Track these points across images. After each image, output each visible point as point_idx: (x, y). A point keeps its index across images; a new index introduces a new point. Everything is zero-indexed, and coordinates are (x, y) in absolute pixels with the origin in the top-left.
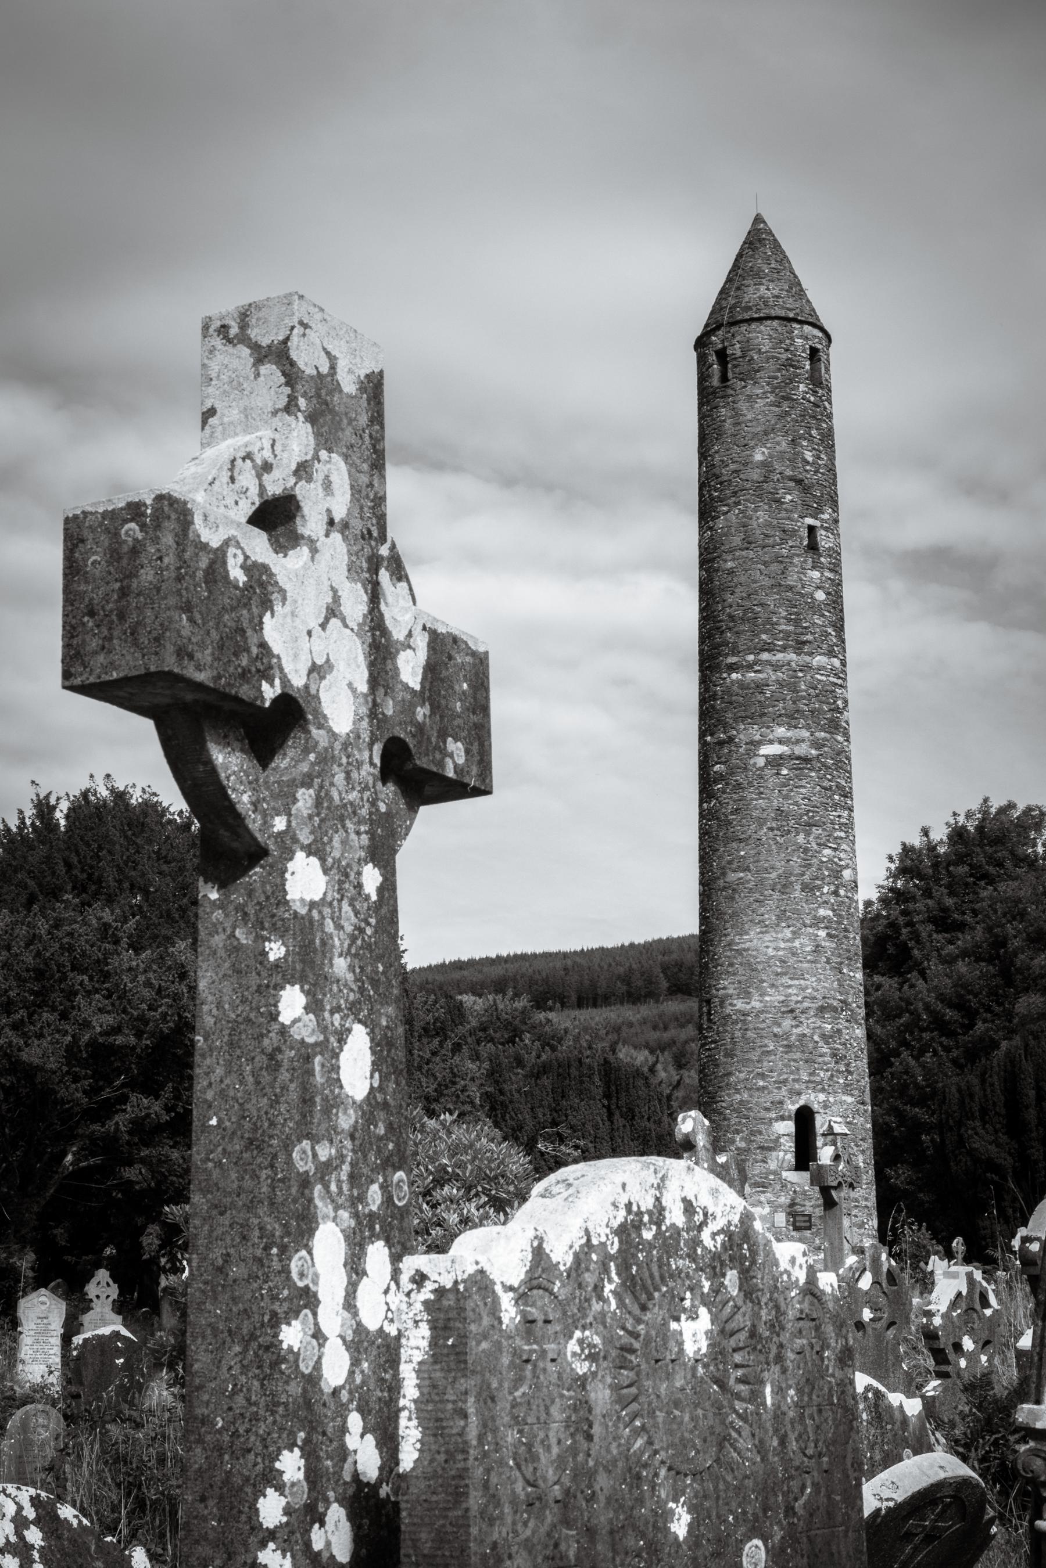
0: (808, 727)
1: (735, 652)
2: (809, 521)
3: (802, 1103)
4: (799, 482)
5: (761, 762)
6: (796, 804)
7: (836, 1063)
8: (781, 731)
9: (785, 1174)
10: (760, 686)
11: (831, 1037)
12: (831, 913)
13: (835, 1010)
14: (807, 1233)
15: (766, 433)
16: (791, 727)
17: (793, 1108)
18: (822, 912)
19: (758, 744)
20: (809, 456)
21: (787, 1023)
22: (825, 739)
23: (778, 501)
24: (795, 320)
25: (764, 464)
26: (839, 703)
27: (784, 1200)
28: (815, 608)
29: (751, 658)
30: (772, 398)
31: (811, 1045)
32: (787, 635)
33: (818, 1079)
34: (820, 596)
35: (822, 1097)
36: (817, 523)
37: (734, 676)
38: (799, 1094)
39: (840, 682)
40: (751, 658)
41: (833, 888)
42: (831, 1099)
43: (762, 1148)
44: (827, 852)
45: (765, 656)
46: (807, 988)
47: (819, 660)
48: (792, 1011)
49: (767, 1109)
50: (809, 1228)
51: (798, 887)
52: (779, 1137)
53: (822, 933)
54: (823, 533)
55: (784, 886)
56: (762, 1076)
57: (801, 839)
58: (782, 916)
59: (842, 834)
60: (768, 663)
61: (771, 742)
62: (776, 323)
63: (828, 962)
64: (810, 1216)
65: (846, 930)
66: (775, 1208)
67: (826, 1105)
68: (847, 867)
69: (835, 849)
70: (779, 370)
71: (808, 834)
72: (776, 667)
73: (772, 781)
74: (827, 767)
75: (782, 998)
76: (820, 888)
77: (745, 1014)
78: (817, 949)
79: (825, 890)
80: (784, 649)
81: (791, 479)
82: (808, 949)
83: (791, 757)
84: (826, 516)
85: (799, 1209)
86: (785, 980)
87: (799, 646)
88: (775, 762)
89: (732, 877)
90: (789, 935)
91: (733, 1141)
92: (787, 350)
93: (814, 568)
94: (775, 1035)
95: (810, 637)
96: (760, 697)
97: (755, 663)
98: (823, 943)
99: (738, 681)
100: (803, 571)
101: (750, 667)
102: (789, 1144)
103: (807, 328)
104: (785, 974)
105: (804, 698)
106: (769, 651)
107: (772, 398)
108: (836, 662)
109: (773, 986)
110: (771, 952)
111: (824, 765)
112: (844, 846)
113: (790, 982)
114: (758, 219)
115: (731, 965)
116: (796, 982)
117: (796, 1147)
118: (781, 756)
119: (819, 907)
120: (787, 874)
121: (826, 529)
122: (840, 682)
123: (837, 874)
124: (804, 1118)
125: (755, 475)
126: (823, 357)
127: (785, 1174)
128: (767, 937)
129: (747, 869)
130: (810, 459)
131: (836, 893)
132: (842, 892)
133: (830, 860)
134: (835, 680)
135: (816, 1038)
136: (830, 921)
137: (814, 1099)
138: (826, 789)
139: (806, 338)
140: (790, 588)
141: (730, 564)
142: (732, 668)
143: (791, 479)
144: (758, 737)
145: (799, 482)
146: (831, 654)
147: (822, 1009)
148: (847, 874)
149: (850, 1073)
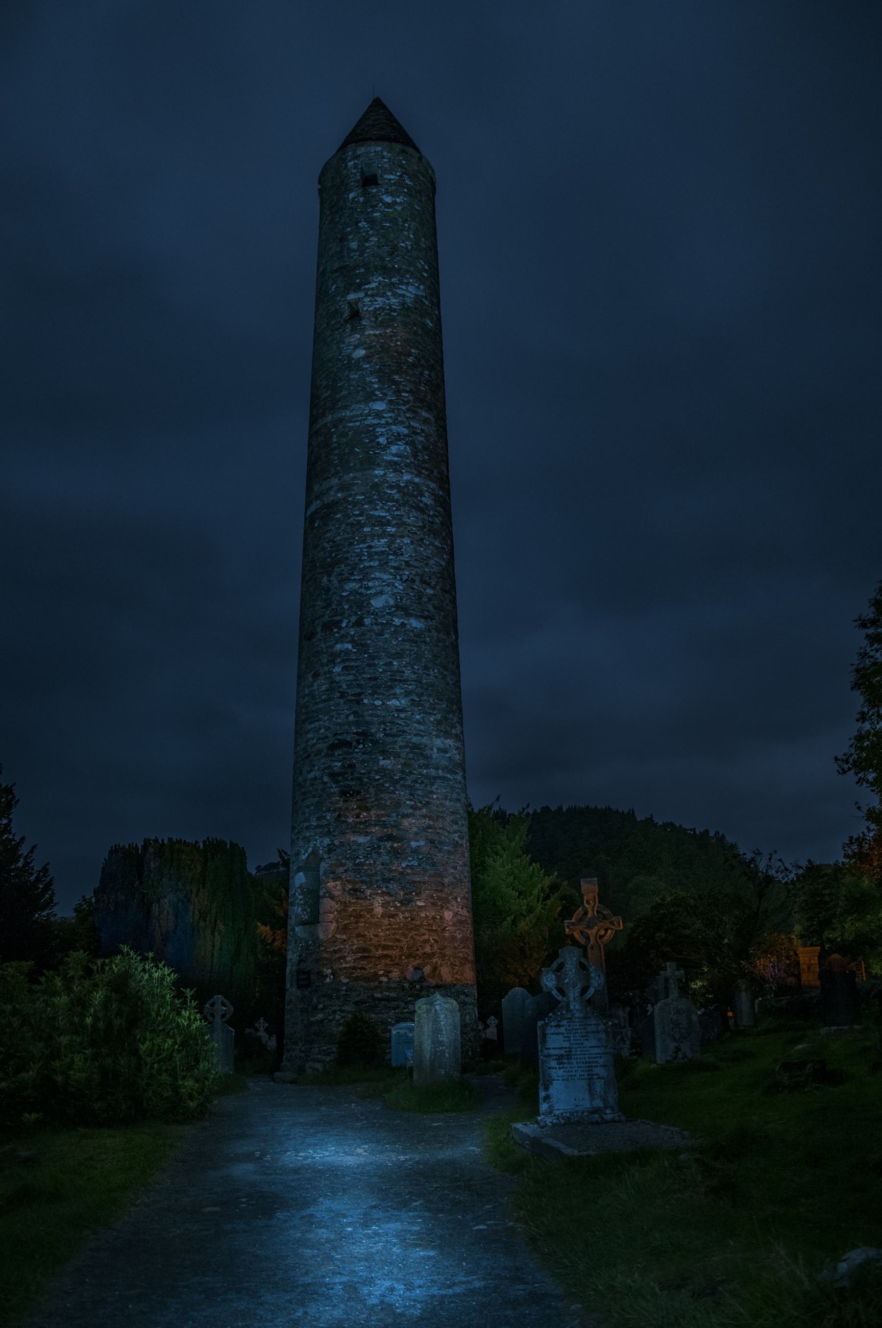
2: (352, 296)
7: (345, 801)
11: (339, 774)
12: (350, 646)
13: (348, 744)
18: (339, 647)
26: (382, 440)
33: (325, 822)
35: (327, 841)
39: (383, 421)
41: (353, 619)
42: (336, 842)
46: (320, 729)
51: (319, 629)
53: (337, 669)
54: (367, 300)
63: (343, 695)
64: (308, 973)
67: (330, 850)
69: (360, 580)
79: (344, 625)
82: (324, 688)
84: (373, 285)
90: (311, 680)
98: (338, 679)
105: (335, 448)
112: (377, 574)
113: (309, 727)
116: (313, 725)
118: (316, 512)
119: (337, 643)
122: (383, 421)
131: (359, 623)
132: (367, 621)
134: (375, 422)
135: (326, 779)
136: (347, 652)
138: (352, 525)
147: (333, 747)
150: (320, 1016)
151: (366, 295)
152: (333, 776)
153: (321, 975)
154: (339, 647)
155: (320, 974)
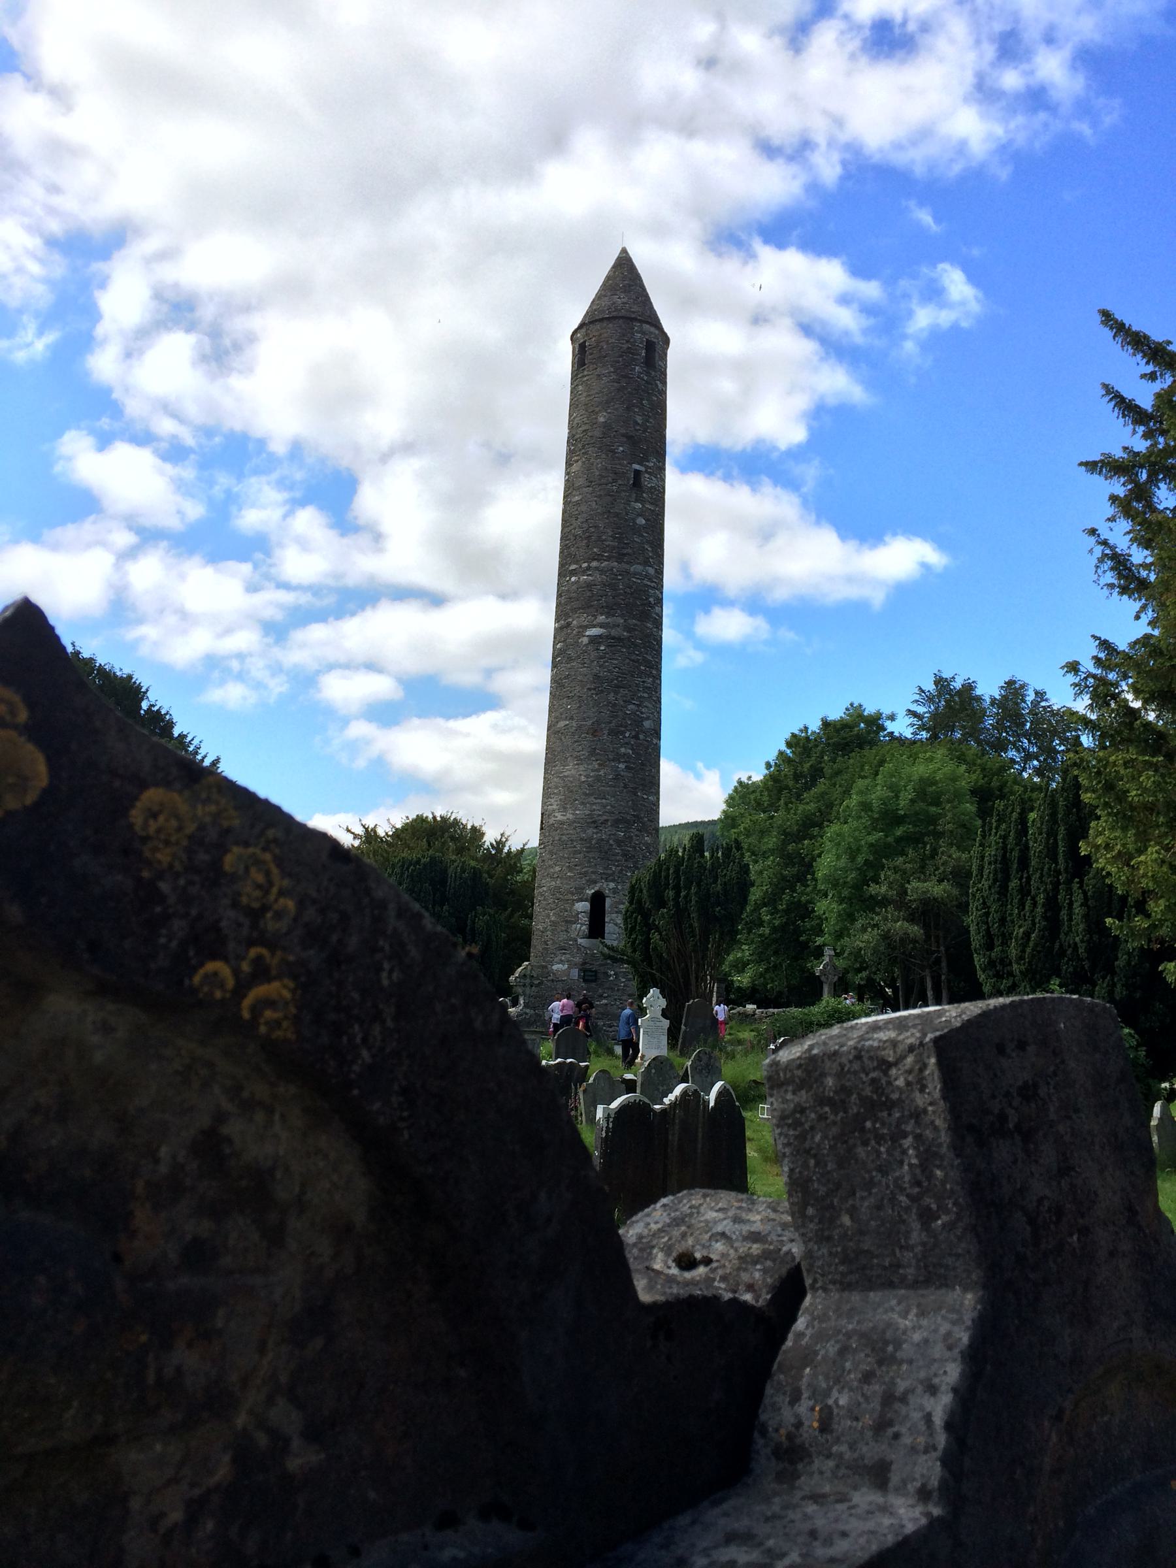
0: (622, 616)
1: (577, 562)
3: (597, 889)
4: (629, 438)
5: (585, 640)
6: (609, 671)
8: (602, 618)
9: (579, 941)
10: (589, 586)
14: (593, 985)
15: (607, 402)
16: (608, 615)
17: (590, 892)
18: (623, 750)
19: (586, 627)
20: (639, 419)
21: (590, 831)
22: (635, 625)
23: (613, 451)
24: (635, 319)
25: (607, 426)
27: (578, 960)
28: (636, 530)
29: (585, 565)
30: (614, 376)
31: (606, 848)
32: (614, 548)
33: (610, 872)
34: (641, 521)
35: (612, 885)
36: (643, 469)
37: (573, 579)
38: (595, 882)
40: (585, 565)
43: (567, 922)
44: (631, 707)
45: (594, 564)
47: (638, 568)
48: (594, 822)
49: (573, 894)
50: (595, 981)
51: (606, 732)
52: (578, 913)
53: (622, 766)
55: (596, 731)
56: (570, 869)
57: (611, 697)
58: (593, 752)
59: (646, 695)
60: (596, 568)
61: (594, 626)
62: (621, 321)
65: (642, 764)
66: (572, 965)
68: (648, 718)
70: (621, 356)
71: (616, 693)
72: (602, 571)
73: (594, 654)
74: (636, 645)
75: (587, 812)
76: (623, 733)
77: (562, 823)
78: (617, 777)
80: (609, 559)
81: (623, 435)
83: (609, 637)
85: (588, 966)
86: (592, 799)
87: (620, 557)
88: (594, 640)
89: (562, 724)
91: (548, 916)
92: (628, 342)
93: (636, 501)
94: (582, 839)
95: (630, 551)
96: (589, 594)
97: (588, 568)
99: (575, 582)
100: (628, 502)
101: (584, 572)
102: (584, 919)
103: (646, 327)
104: (591, 795)
105: (621, 594)
106: (598, 560)
107: (614, 376)
108: (651, 571)
109: (582, 803)
110: (583, 779)
111: (633, 643)
112: (646, 704)
114: (624, 251)
115: (557, 787)
117: (590, 921)
118: (600, 636)
120: (598, 722)
121: (649, 473)
123: (638, 722)
124: (598, 901)
125: (597, 433)
126: (658, 347)
127: (579, 941)
128: (582, 768)
129: (572, 718)
130: (640, 422)
131: (636, 737)
132: (641, 737)
133: (634, 713)
136: (629, 756)
137: (608, 887)
139: (644, 333)
140: (617, 515)
141: (577, 498)
142: (573, 573)
143: (623, 435)
144: (586, 623)
145: (629, 438)
146: (646, 563)
147: (616, 822)
148: (647, 724)
149: (637, 868)
150: (604, 1001)
151: (646, 472)
152: (619, 842)
153: (607, 975)
154: (623, 750)
155: (606, 973)
